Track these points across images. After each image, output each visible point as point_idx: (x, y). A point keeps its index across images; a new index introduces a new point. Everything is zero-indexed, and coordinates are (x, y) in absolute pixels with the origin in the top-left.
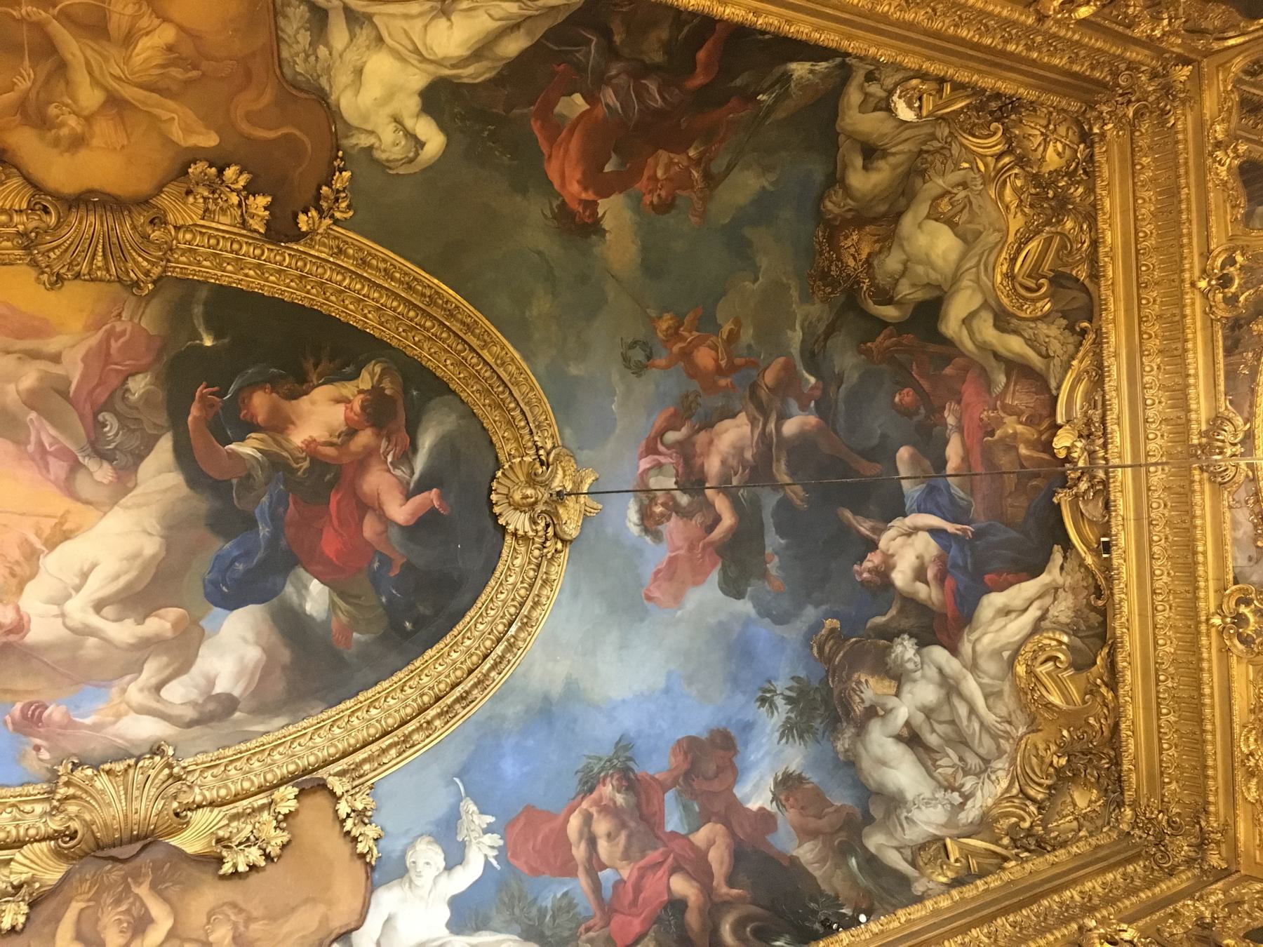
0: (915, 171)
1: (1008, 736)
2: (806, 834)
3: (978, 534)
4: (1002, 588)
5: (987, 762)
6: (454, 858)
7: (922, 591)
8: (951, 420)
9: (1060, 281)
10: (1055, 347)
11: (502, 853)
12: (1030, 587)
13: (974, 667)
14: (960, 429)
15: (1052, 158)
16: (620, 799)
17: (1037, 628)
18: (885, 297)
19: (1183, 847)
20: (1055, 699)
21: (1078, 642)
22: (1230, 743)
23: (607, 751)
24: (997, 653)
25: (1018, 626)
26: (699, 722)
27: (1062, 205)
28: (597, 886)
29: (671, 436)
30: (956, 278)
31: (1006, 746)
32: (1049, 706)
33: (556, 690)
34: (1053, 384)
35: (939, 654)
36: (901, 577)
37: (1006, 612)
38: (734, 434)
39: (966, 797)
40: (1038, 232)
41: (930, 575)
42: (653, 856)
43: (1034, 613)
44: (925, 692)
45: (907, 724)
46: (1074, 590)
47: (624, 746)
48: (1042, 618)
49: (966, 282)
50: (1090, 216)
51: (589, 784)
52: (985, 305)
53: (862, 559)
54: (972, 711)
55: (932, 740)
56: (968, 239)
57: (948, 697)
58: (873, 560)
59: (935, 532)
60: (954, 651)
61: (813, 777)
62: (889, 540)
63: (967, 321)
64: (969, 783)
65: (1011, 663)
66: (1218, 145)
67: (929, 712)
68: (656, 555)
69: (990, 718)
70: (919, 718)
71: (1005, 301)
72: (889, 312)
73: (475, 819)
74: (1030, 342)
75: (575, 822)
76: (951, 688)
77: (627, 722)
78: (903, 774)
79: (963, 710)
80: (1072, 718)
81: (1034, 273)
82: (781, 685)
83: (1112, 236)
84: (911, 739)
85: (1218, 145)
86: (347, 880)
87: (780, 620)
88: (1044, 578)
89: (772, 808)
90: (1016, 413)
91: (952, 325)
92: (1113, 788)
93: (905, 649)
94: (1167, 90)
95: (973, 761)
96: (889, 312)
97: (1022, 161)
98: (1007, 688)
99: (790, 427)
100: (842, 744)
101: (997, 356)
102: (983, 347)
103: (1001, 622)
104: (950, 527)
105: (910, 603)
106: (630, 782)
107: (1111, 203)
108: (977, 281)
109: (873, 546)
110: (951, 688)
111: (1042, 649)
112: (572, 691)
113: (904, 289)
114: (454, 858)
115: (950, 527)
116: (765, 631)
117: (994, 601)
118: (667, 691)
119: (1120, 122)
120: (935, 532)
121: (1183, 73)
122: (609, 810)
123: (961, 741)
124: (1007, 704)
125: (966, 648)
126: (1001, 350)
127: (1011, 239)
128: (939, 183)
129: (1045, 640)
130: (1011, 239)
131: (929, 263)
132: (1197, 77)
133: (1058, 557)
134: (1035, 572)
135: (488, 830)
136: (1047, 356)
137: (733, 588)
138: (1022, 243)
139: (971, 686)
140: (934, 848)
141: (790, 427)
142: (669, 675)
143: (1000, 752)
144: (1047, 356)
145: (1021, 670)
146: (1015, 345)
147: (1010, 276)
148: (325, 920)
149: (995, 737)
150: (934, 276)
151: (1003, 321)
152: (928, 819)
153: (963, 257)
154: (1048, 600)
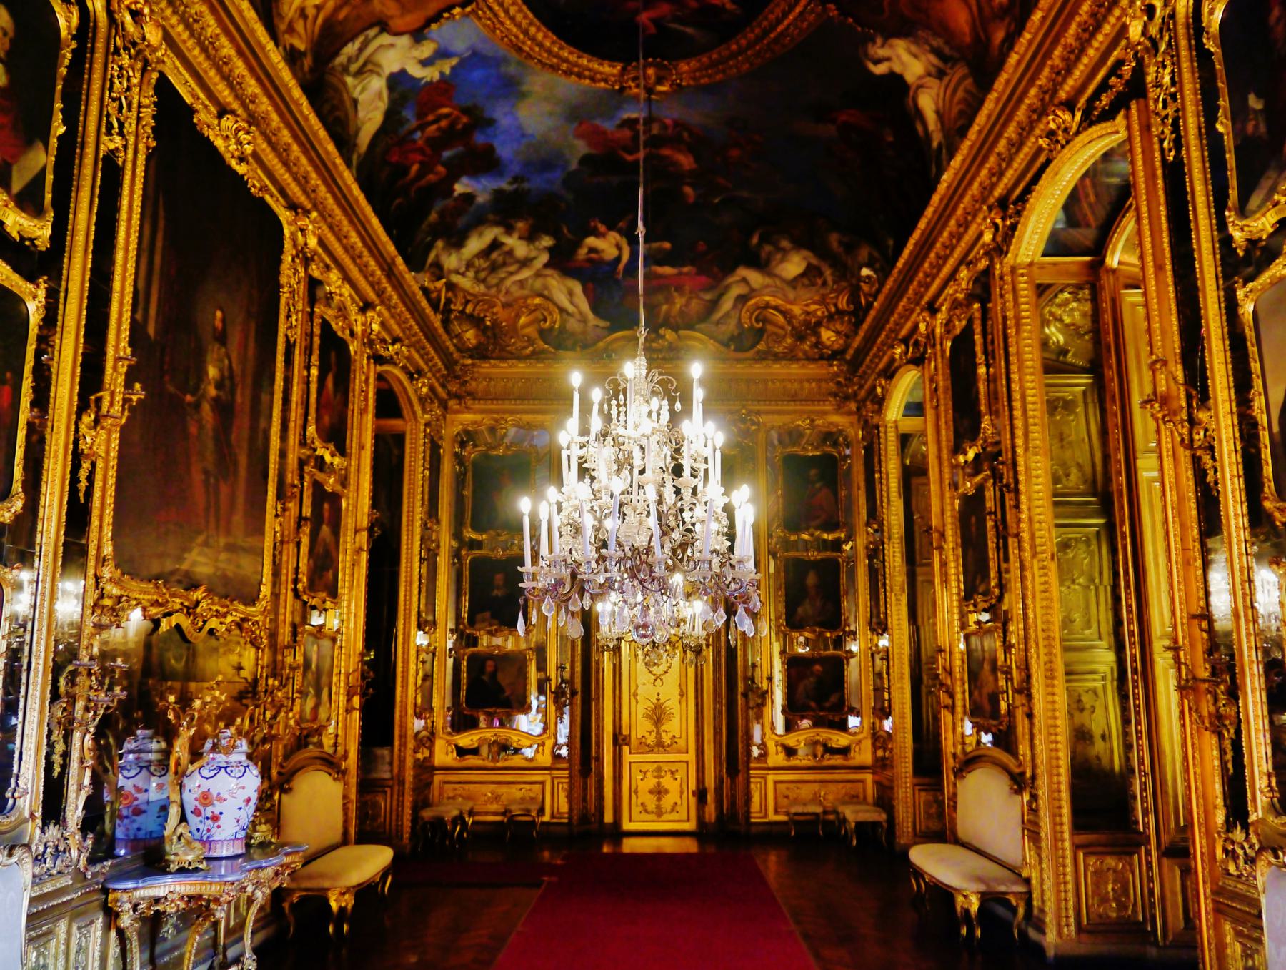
0: (835, 263)
1: (499, 291)
2: (442, 214)
3: (617, 281)
4: (585, 291)
5: (484, 281)
6: (425, 63)
7: (583, 252)
8: (686, 269)
9: (760, 333)
10: (723, 328)
11: (430, 84)
12: (585, 306)
13: (538, 275)
14: (680, 274)
15: (827, 335)
16: (459, 126)
17: (562, 310)
18: (763, 240)
19: (454, 388)
20: (523, 320)
21: (556, 333)
22: (512, 412)
23: (486, 115)
24: (546, 287)
25: (563, 300)
26: (504, 151)
27: (800, 337)
28: (414, 131)
29: (685, 135)
30: (771, 274)
31: (493, 291)
32: (518, 316)
33: (525, 88)
34: (702, 326)
35: (545, 258)
36: (591, 241)
37: (571, 293)
38: (685, 161)
39: (463, 275)
40: (789, 322)
41: (593, 256)
42: (428, 151)
43: (571, 308)
44: (521, 249)
45: (503, 244)
46: (584, 333)
47: (491, 122)
48: (568, 313)
49: (768, 281)
50: (790, 356)
51: (466, 111)
52: (753, 290)
53: (603, 223)
54: (511, 274)
55: (494, 256)
56: (793, 283)
57: (517, 261)
58: (602, 228)
59: (618, 259)
60: (546, 266)
61: (472, 209)
62: (614, 236)
63: (744, 280)
64: (471, 274)
65: (541, 295)
66: (812, 421)
67: (510, 253)
68: (608, 126)
69: (508, 283)
70: (506, 249)
71: (753, 301)
72: (755, 240)
73: (446, 67)
74: (727, 315)
75: (445, 110)
76: (525, 263)
77: (504, 122)
78: (475, 244)
79: (512, 268)
80: (514, 330)
81: (766, 321)
82: (526, 186)
83: (777, 368)
84: (495, 245)
85: (812, 421)
86: (413, 20)
87: (564, 182)
88: (591, 316)
89: (456, 194)
90: (687, 304)
91: (743, 272)
92: (480, 353)
93: (547, 241)
94: (847, 398)
95: (483, 275)
96: (755, 240)
97: (831, 317)
98: (525, 292)
99: (688, 190)
100: (491, 217)
101: (721, 295)
102: (728, 288)
103: (565, 291)
104: (621, 266)
105: (578, 244)
106: (469, 130)
107: (795, 369)
108: (767, 286)
109: (611, 227)
110: (525, 263)
111: (550, 314)
112: (523, 95)
113: (768, 248)
114: (425, 63)
115: (621, 266)
116: (558, 176)
117: (577, 288)
118: (523, 135)
119: (836, 375)
120: (618, 259)
121: (853, 406)
122: (452, 125)
123: (494, 268)
124: (516, 292)
125: (549, 272)
126: (725, 297)
127: (789, 306)
128: (828, 273)
129: (557, 316)
130: (789, 306)
131: (782, 261)
132: (850, 413)
133: (602, 323)
134: (595, 310)
135: (442, 74)
136: (718, 323)
137: (585, 160)
138: (784, 313)
139: (526, 274)
140: (438, 271)
141: (688, 190)
142: (532, 136)
143: (489, 287)
144: (718, 323)
145: (537, 300)
146: (727, 304)
147: (768, 306)
148: (392, 17)
149: (498, 285)
150: (774, 263)
151: (742, 299)
152: (451, 261)
153: (783, 280)
154: (578, 316)
